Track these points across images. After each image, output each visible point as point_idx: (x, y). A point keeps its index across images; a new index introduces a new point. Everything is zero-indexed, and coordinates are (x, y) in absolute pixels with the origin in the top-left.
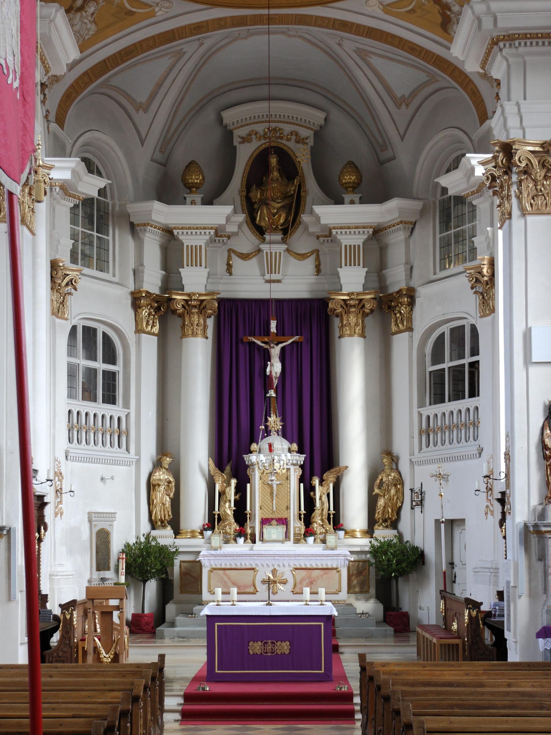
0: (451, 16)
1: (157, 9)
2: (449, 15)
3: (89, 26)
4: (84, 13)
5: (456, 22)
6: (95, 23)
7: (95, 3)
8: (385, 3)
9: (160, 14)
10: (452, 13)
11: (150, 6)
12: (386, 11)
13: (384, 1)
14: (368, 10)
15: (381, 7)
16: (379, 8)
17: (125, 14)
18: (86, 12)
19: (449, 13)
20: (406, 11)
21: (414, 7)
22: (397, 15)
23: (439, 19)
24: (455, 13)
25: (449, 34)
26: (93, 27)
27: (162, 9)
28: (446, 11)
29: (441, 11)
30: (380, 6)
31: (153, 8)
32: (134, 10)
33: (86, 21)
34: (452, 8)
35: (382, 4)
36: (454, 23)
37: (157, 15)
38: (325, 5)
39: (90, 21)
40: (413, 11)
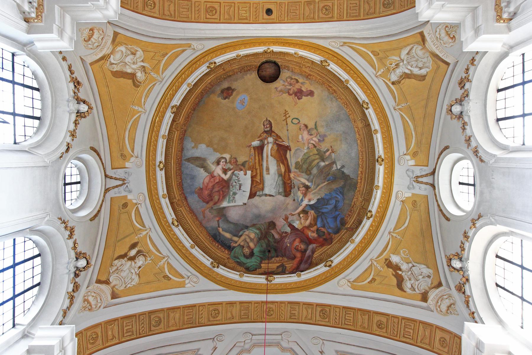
0: (402, 274)
1: (187, 281)
2: (401, 274)
3: (134, 276)
4: (133, 263)
5: (408, 279)
6: (139, 277)
7: (144, 258)
8: (351, 280)
9: (189, 287)
10: (403, 272)
11: (183, 277)
12: (354, 288)
13: (351, 278)
14: (340, 290)
15: (349, 284)
16: (348, 285)
17: (164, 277)
18: (135, 263)
19: (400, 273)
20: (368, 282)
21: (374, 276)
22: (362, 288)
23: (394, 281)
24: (405, 271)
25: (405, 292)
26: (136, 279)
27: (191, 282)
28: (398, 271)
29: (394, 273)
30: (348, 283)
31: (184, 279)
32: (170, 276)
33: (133, 271)
34: (402, 267)
35: (349, 281)
36: (407, 280)
37: (186, 286)
38: (308, 290)
39: (136, 272)
40: (373, 280)
